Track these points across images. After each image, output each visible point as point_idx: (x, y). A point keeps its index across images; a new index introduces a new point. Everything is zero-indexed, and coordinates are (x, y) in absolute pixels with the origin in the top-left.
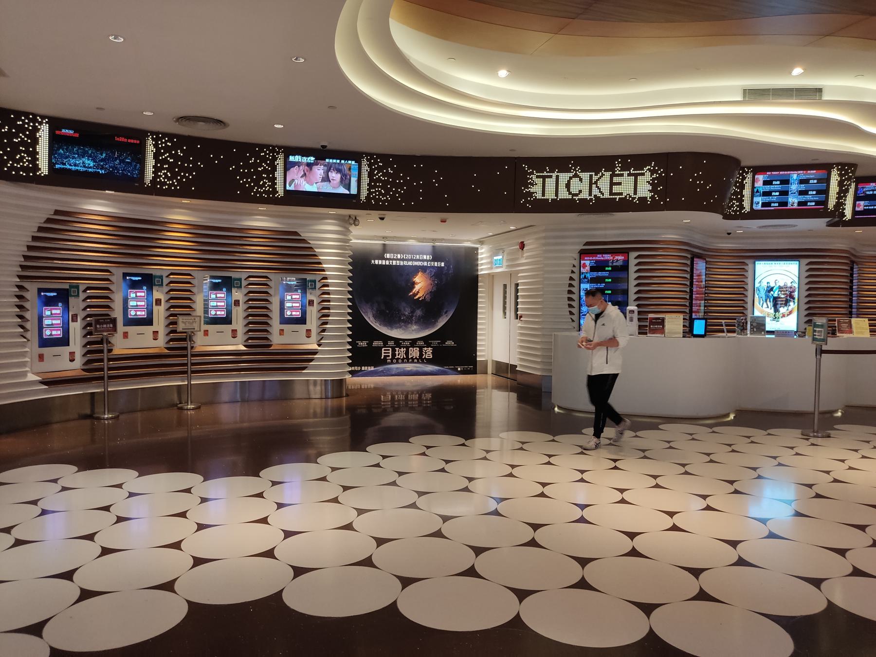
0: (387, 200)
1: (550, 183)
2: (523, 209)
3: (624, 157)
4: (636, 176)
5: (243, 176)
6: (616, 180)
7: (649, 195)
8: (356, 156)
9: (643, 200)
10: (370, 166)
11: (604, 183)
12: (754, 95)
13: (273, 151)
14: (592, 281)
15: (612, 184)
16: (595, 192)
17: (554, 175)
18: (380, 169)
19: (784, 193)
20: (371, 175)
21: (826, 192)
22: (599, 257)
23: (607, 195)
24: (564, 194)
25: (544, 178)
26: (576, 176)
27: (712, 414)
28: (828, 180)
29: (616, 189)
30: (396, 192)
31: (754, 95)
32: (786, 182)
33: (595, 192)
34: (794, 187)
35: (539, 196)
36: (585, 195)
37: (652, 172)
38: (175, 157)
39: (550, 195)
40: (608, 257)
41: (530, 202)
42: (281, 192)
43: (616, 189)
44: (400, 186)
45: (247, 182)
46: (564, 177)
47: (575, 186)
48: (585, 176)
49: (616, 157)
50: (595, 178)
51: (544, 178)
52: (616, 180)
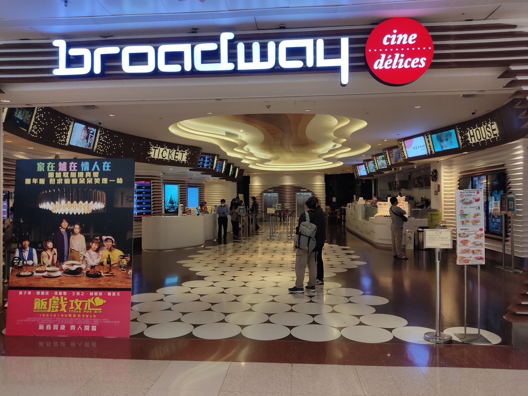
0: (101, 152)
1: (157, 151)
2: (145, 161)
3: (180, 145)
4: (183, 153)
5: (59, 132)
6: (177, 153)
7: (185, 161)
8: (96, 127)
9: (183, 162)
10: (100, 133)
11: (173, 154)
12: (228, 134)
13: (70, 120)
14: (138, 193)
15: (176, 155)
16: (170, 157)
17: (159, 148)
18: (103, 135)
19: (204, 162)
20: (100, 138)
21: (213, 163)
22: (140, 182)
23: (173, 159)
24: (160, 157)
25: (155, 149)
26: (165, 150)
27: (192, 245)
28: (214, 160)
29: (176, 157)
30: (106, 148)
31: (228, 134)
32: (204, 159)
33: (170, 157)
34: (206, 161)
35: (152, 156)
36: (167, 158)
37: (188, 152)
38: (40, 117)
39: (156, 157)
40: (143, 182)
41: (148, 158)
42: (67, 144)
43: (176, 157)
44: (108, 145)
45: (58, 136)
46: (162, 149)
47: (166, 154)
48: (168, 150)
49: (178, 145)
50: (171, 152)
51: (155, 149)
52: (177, 153)
